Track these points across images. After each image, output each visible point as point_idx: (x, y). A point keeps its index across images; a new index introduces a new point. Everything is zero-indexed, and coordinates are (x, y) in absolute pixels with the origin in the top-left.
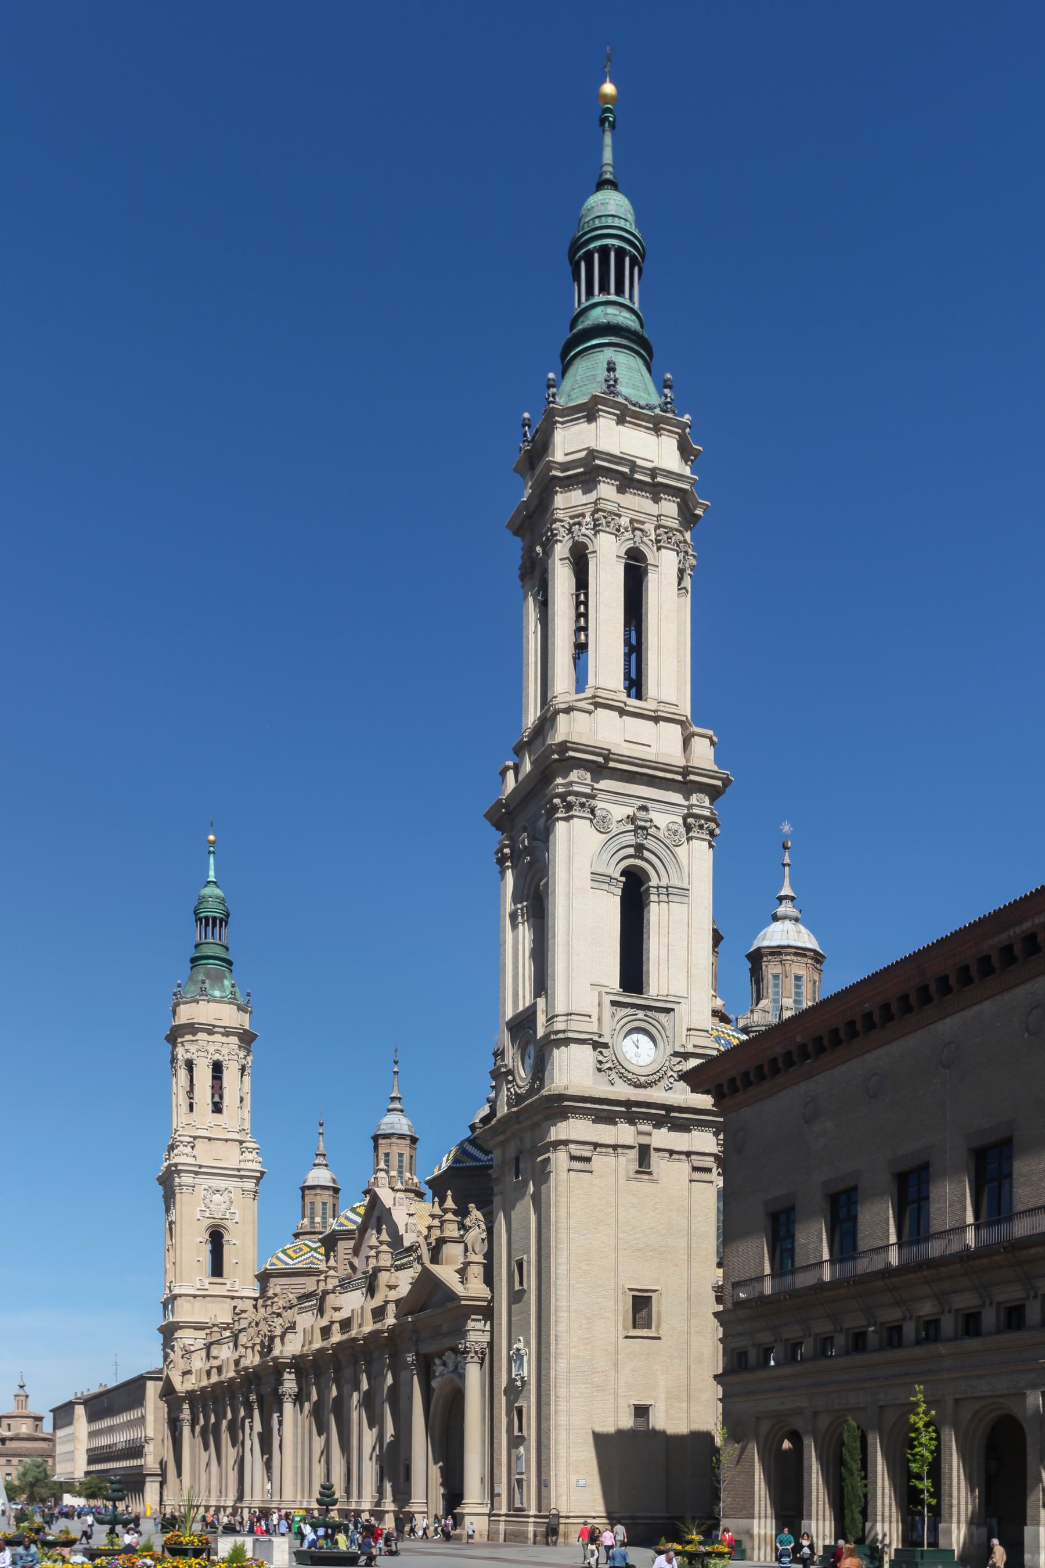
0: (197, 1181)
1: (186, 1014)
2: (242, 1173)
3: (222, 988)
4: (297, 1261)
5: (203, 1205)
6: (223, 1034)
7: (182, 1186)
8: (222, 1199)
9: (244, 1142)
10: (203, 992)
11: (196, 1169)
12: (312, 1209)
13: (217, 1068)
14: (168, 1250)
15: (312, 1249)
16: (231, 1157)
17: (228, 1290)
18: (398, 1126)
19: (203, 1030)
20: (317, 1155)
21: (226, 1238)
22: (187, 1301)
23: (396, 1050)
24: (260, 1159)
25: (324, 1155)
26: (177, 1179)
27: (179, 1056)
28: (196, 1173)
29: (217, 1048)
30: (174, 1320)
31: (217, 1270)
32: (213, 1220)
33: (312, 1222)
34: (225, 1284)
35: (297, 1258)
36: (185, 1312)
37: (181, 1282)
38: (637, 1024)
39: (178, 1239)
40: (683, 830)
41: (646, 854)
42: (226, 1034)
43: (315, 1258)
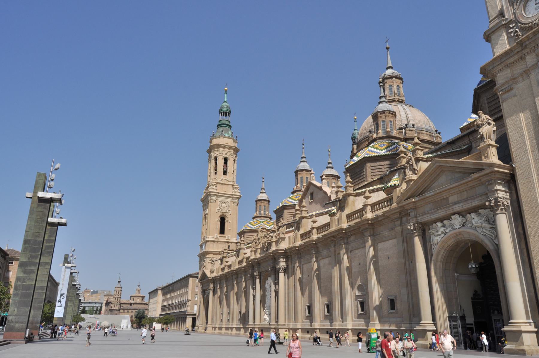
1: (215, 142)
2: (233, 196)
3: (228, 134)
4: (255, 226)
8: (225, 205)
10: (222, 134)
11: (217, 194)
12: (260, 208)
13: (226, 160)
14: (204, 225)
15: (261, 222)
16: (229, 191)
18: (306, 167)
20: (262, 189)
21: (226, 220)
22: (211, 243)
23: (303, 140)
24: (240, 191)
25: (264, 189)
26: (209, 198)
27: (212, 156)
28: (217, 195)
30: (206, 250)
33: (260, 213)
34: (225, 237)
36: (210, 248)
39: (209, 219)
42: (229, 149)
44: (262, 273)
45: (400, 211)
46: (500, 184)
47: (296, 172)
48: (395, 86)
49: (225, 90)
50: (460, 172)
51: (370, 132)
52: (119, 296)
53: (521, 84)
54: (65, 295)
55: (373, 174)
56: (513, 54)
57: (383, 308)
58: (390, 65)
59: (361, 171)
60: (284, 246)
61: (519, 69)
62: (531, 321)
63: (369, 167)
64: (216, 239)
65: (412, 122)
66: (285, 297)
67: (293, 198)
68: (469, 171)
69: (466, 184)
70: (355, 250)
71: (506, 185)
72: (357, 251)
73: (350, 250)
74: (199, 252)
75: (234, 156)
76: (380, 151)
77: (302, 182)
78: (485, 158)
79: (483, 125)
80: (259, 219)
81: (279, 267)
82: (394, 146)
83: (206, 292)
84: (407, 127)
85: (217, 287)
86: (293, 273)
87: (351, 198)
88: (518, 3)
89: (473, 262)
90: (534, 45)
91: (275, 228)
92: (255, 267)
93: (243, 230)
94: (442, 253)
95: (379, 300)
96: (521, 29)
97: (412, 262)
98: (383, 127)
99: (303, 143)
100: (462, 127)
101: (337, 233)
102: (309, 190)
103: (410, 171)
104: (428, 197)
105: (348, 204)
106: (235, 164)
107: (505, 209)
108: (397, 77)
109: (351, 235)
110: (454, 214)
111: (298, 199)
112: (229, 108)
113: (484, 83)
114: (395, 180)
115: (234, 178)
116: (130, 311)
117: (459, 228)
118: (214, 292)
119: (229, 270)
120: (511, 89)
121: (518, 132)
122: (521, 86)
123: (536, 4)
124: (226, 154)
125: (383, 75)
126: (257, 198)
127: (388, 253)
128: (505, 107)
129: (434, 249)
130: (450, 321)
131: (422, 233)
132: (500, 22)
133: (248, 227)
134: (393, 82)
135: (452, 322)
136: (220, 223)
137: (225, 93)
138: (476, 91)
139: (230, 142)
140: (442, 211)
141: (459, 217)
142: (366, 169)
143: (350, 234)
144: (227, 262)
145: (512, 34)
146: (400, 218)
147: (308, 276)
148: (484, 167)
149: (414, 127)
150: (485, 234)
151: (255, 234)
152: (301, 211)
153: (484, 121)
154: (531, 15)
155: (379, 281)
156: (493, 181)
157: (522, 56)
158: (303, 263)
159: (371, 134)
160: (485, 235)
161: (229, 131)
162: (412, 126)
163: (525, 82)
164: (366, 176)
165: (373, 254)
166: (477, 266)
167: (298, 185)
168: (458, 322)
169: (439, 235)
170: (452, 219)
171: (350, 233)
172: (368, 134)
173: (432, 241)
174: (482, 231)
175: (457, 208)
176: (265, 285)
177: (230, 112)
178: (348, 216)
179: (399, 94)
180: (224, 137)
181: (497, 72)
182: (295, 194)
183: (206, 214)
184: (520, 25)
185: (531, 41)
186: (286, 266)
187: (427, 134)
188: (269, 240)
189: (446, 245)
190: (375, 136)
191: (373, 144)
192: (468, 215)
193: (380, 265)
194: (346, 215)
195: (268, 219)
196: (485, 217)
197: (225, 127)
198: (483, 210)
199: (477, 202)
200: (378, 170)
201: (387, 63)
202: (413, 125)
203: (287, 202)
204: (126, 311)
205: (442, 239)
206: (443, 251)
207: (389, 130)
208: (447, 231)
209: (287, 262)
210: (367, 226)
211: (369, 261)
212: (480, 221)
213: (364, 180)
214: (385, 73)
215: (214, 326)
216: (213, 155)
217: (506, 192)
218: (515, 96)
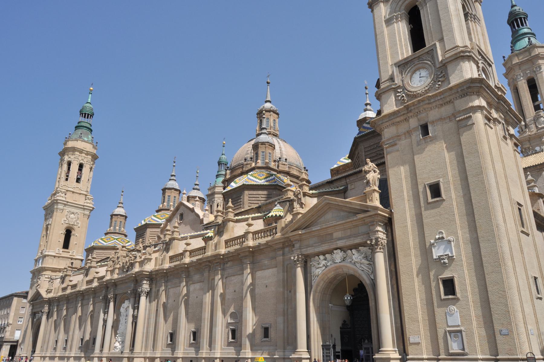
1: (70, 144)
2: (85, 207)
3: (88, 138)
4: (107, 243)
5: (66, 218)
6: (86, 154)
7: (58, 209)
9: (87, 195)
10: (80, 137)
11: (66, 203)
12: (115, 223)
13: (81, 166)
14: (43, 237)
15: (115, 239)
16: (81, 201)
17: (70, 255)
18: (175, 186)
19: (78, 151)
20: (119, 203)
21: (73, 233)
23: (175, 158)
25: (122, 203)
26: (56, 207)
27: (65, 159)
28: (66, 204)
29: (82, 158)
30: (43, 266)
32: (68, 225)
34: (69, 252)
35: (108, 242)
36: (49, 263)
37: (49, 249)
39: (51, 231)
43: (116, 242)
44: (118, 295)
45: (284, 241)
46: (380, 226)
47: (164, 190)
48: (272, 120)
49: (90, 90)
50: (346, 211)
51: (245, 160)
53: (403, 142)
55: (250, 201)
56: (400, 115)
57: (256, 336)
58: (269, 99)
59: (238, 197)
60: (149, 267)
61: (403, 128)
62: (397, 349)
63: (247, 195)
64: (57, 254)
65: (285, 156)
66: (144, 323)
67: (159, 216)
68: (355, 211)
69: (351, 223)
70: (231, 276)
71: (384, 227)
72: (233, 278)
73: (225, 276)
74: (33, 268)
75: (92, 163)
76: (259, 181)
77: (169, 201)
78: (370, 201)
79: (370, 171)
80: (112, 235)
81: (142, 290)
82: (272, 177)
83: (37, 315)
84: (280, 161)
85: (53, 309)
86: (157, 297)
87: (231, 224)
88: (406, 73)
89: (348, 294)
90: (417, 111)
91: (141, 247)
92: (109, 289)
93: (93, 246)
94: (321, 285)
95: (253, 327)
96: (407, 95)
97: (290, 292)
98: (262, 158)
99: (175, 161)
100: (332, 168)
101: (214, 258)
102: (179, 211)
103: (298, 204)
104: (314, 231)
105: (227, 229)
107: (383, 248)
108: (274, 112)
109: (229, 261)
110: (336, 249)
111: (163, 218)
112: (92, 109)
113: (363, 133)
114: (276, 210)
117: (340, 262)
118: (49, 316)
119: (73, 291)
120: (395, 144)
121: (398, 182)
122: (403, 143)
123: (420, 77)
124: (82, 160)
125: (262, 107)
126: (113, 213)
127: (266, 282)
128: (389, 159)
129: (314, 280)
130: (323, 349)
131: (305, 264)
132: (391, 85)
133: (98, 243)
134: (270, 116)
135: (325, 350)
136: (64, 236)
137: (90, 93)
138: (356, 139)
139: (89, 147)
140: (326, 245)
141: (341, 252)
142: (244, 197)
143: (227, 260)
144: (71, 281)
145: (399, 98)
146: (283, 248)
147: (174, 301)
148: (369, 210)
149: (286, 162)
150: (363, 269)
151: (113, 252)
152: (173, 232)
153: (371, 168)
154: (415, 86)
155: (254, 309)
156: (375, 223)
157: (406, 118)
158: (169, 287)
159: (246, 162)
160: (363, 270)
162: (284, 160)
163: (407, 140)
164: (243, 203)
165: (251, 281)
166: (352, 298)
167: (165, 204)
168: (331, 350)
169: (320, 267)
170: (334, 253)
171: (228, 259)
172: (242, 161)
173: (312, 272)
174: (361, 266)
175: (340, 243)
176: (119, 309)
177: (93, 115)
178: (226, 242)
179: (275, 128)
180: (82, 141)
181: (385, 128)
182: (160, 213)
183: (48, 224)
184: (406, 91)
185: (415, 107)
186: (149, 290)
187: (296, 170)
188: (131, 260)
189: (326, 278)
190: (253, 165)
191: (252, 173)
192: (349, 251)
193: (256, 293)
194: (225, 241)
195: (123, 236)
196: (364, 254)
197: (84, 130)
198: (363, 247)
199: (359, 240)
200: (256, 199)
201: (267, 97)
202: (286, 160)
203: (152, 220)
205: (323, 272)
206: (322, 282)
207: (268, 161)
208: (328, 264)
209: (150, 285)
210: (247, 254)
211: (246, 289)
212: (359, 257)
213: (241, 207)
214: (263, 106)
215: (43, 355)
216: (66, 158)
217: (384, 233)
218: (398, 151)
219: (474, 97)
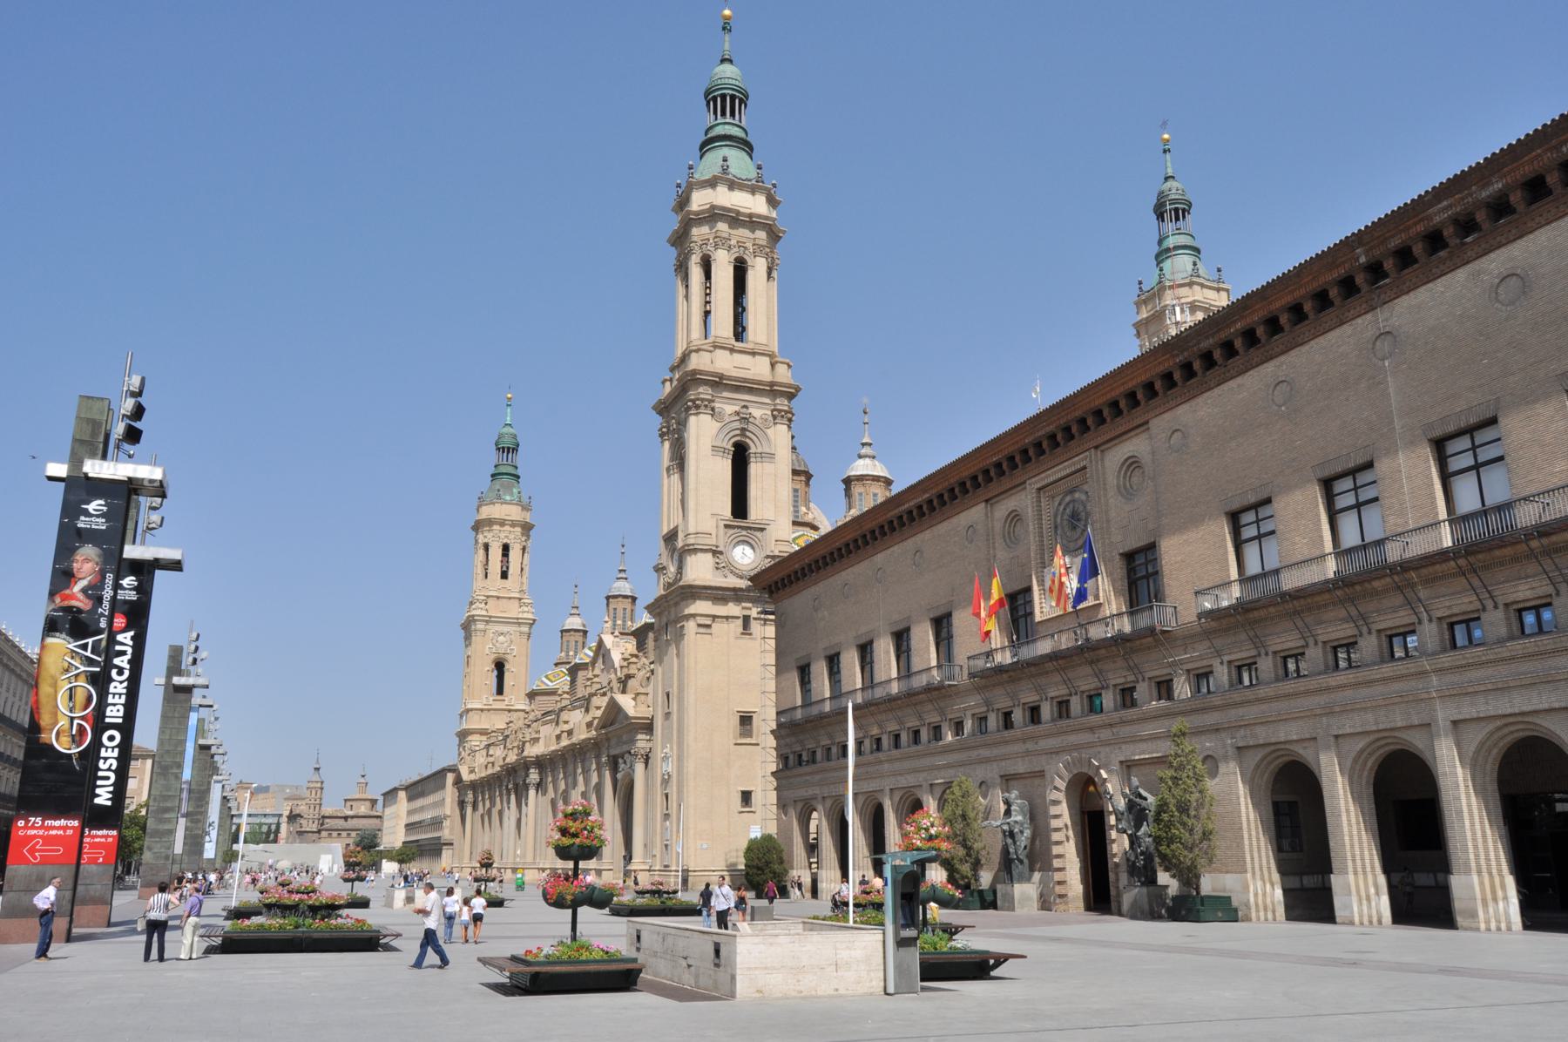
0: (488, 627)
1: (487, 512)
3: (512, 494)
10: (499, 497)
13: (506, 548)
16: (513, 610)
21: (507, 666)
26: (473, 627)
27: (480, 541)
28: (487, 621)
31: (500, 691)
33: (568, 655)
36: (474, 723)
38: (742, 538)
40: (771, 418)
41: (748, 433)
52: (318, 802)
54: (216, 825)
106: (526, 555)
112: (515, 436)
115: (522, 583)
116: (344, 834)
124: (506, 537)
139: (514, 513)
161: (514, 486)
177: (518, 445)
180: (502, 503)
197: (505, 479)
204: (335, 834)
219: (690, 601)
